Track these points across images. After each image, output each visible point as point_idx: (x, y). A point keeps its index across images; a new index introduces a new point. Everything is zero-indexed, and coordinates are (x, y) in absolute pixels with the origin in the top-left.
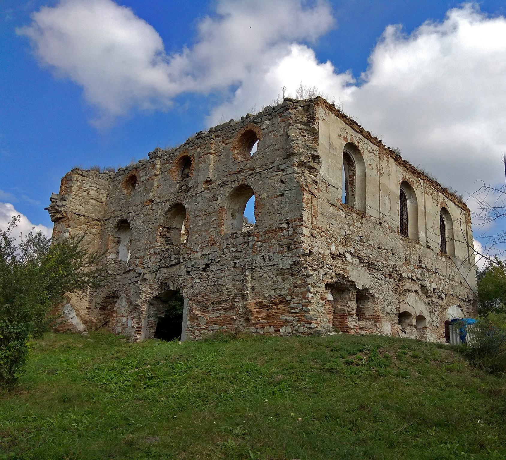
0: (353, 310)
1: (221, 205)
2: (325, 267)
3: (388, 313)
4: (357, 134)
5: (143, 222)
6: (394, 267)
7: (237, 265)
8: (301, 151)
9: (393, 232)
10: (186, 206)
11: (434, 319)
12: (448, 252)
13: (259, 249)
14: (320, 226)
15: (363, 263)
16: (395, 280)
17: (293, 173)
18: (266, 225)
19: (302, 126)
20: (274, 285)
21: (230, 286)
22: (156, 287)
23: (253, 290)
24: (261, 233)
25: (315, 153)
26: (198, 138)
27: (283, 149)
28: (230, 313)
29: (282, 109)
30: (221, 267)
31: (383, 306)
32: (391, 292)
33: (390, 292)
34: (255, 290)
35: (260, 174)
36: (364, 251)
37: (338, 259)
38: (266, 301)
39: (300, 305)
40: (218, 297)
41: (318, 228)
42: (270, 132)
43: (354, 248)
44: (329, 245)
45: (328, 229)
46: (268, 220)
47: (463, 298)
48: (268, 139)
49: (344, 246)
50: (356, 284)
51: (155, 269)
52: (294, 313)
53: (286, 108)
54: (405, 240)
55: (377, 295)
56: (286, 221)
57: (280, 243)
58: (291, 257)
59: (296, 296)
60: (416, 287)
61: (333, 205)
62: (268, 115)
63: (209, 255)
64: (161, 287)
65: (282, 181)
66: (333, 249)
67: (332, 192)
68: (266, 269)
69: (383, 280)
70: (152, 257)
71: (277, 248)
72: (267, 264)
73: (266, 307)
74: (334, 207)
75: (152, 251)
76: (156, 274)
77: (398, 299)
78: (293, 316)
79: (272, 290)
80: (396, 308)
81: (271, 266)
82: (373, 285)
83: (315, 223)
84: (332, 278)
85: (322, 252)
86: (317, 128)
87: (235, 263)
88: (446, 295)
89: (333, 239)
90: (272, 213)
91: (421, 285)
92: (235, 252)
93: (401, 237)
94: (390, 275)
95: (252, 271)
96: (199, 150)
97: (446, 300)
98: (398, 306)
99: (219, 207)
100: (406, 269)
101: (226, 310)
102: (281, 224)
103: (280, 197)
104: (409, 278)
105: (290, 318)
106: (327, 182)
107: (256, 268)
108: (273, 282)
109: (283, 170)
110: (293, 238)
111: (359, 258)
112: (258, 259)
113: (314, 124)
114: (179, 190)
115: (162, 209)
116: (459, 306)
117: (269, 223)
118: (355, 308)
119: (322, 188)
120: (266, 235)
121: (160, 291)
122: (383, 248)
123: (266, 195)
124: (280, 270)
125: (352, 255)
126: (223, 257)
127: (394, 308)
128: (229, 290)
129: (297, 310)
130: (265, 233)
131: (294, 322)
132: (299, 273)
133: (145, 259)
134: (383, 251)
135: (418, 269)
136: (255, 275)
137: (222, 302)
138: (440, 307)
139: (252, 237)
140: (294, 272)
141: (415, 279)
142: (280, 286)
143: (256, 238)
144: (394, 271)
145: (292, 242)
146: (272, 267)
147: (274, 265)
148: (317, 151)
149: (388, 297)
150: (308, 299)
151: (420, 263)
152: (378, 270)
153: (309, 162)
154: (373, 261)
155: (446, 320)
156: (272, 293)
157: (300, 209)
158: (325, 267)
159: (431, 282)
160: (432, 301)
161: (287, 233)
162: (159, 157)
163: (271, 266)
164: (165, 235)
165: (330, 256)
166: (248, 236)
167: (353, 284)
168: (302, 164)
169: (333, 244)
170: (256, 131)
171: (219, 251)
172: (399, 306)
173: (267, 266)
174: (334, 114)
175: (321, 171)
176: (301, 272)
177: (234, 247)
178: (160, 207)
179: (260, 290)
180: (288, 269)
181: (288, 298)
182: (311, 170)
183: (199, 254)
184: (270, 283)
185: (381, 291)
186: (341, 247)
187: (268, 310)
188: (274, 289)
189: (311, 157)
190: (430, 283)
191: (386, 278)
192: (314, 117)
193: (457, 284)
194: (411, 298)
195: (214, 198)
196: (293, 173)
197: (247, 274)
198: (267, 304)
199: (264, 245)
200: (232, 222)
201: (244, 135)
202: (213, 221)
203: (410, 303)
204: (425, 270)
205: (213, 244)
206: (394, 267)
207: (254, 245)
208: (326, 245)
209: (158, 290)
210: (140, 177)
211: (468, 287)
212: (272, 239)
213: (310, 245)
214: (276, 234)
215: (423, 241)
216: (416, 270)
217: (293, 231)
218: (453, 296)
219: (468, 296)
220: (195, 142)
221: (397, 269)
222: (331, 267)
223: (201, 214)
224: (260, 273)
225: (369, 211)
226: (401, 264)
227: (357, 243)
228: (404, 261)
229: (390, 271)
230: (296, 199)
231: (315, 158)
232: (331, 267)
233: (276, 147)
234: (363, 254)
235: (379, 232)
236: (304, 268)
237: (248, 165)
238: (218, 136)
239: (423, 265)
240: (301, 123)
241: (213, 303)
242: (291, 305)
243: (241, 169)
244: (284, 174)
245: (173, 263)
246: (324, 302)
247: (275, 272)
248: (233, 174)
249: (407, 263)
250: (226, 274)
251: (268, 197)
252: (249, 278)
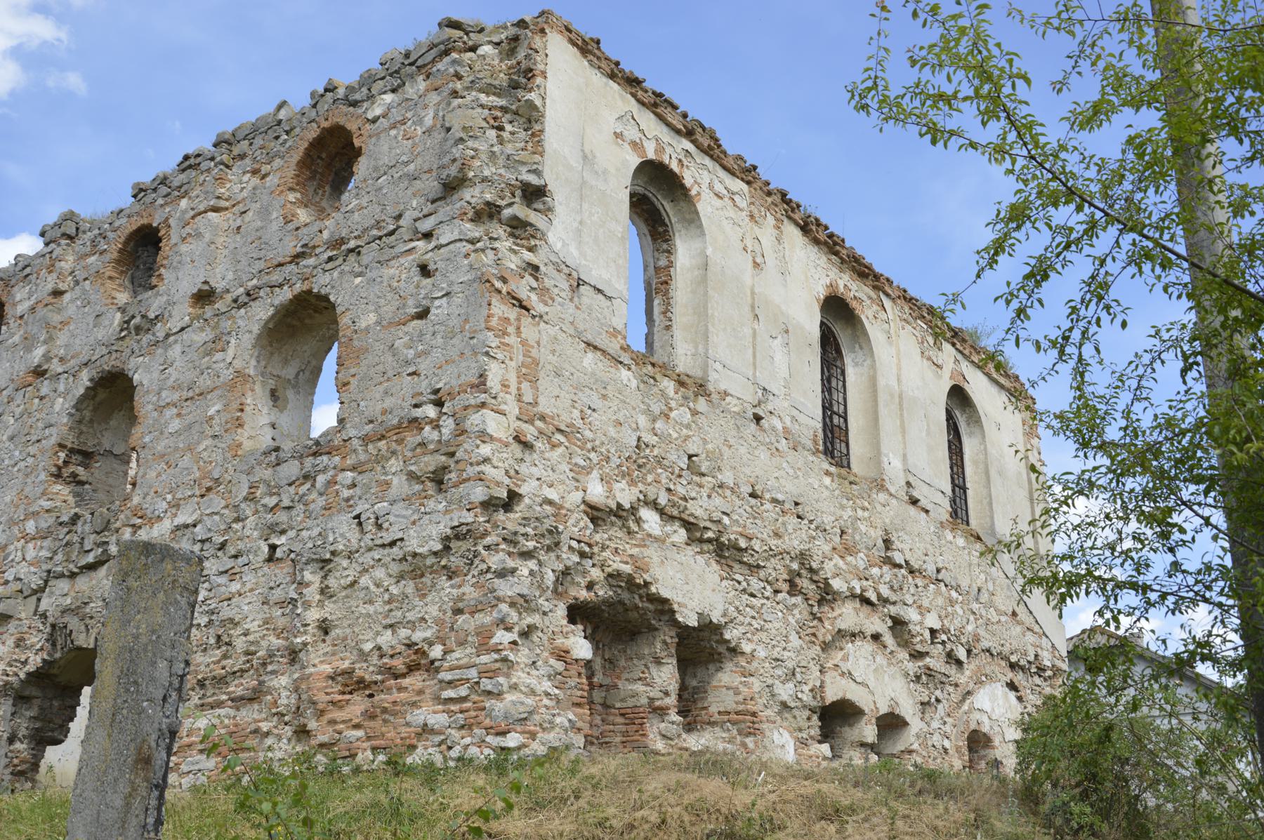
0: (667, 694)
1: (238, 364)
2: (565, 549)
3: (784, 705)
4: (677, 137)
5: (11, 438)
6: (803, 557)
7: (279, 554)
8: (487, 173)
9: (800, 448)
10: (136, 377)
11: (935, 724)
12: (973, 521)
13: (346, 493)
14: (548, 411)
15: (701, 541)
16: (807, 599)
17: (461, 240)
18: (369, 414)
19: (492, 98)
20: (391, 610)
21: (256, 623)
22: (37, 640)
23: (326, 633)
24: (355, 442)
25: (533, 179)
26: (184, 170)
27: (430, 171)
28: (249, 715)
29: (434, 52)
30: (230, 563)
31: (770, 682)
32: (793, 637)
33: (791, 638)
34: (333, 634)
35: (359, 253)
36: (704, 501)
37: (613, 524)
38: (365, 665)
39: (473, 673)
40: (219, 662)
41: (543, 418)
42: (393, 127)
43: (669, 490)
44: (580, 473)
45: (579, 423)
46: (378, 396)
47: (1022, 663)
48: (386, 148)
49: (633, 483)
50: (676, 607)
51: (36, 582)
52: (451, 700)
53: (442, 47)
54: (840, 476)
55: (747, 647)
56: (433, 397)
57: (413, 468)
58: (447, 512)
59: (462, 643)
60: (876, 624)
61: (596, 348)
62: (391, 75)
63: (195, 526)
64: (52, 640)
65: (425, 271)
66: (596, 491)
67: (590, 308)
68: (367, 559)
69: (768, 598)
70: (31, 545)
71: (399, 485)
72: (370, 543)
73: (367, 687)
74: (599, 353)
75: (30, 526)
76: (39, 600)
77: (816, 659)
78: (448, 712)
79: (385, 627)
80: (811, 690)
81: (383, 546)
82: (735, 614)
83: (528, 397)
84: (590, 586)
85: (552, 494)
86: (538, 102)
87: (273, 548)
88: (969, 652)
89: (593, 455)
90: (390, 373)
91: (891, 617)
92: (272, 509)
93: (826, 466)
94: (791, 583)
95: (322, 568)
96: (184, 203)
97: (972, 666)
98: (818, 684)
99: (231, 370)
100: (844, 567)
101: (238, 701)
102: (416, 406)
103: (415, 322)
104: (853, 596)
105: (438, 719)
106: (575, 274)
107: (336, 559)
108: (389, 602)
109: (428, 236)
110: (452, 449)
111: (689, 526)
112: (343, 531)
113: (531, 90)
114: (122, 330)
115: (65, 395)
116: (1012, 686)
117: (379, 407)
118: (673, 687)
119: (556, 291)
120: (370, 446)
121: (49, 654)
122: (767, 496)
123: (372, 318)
124: (409, 558)
125: (661, 512)
126: (237, 531)
127: (806, 688)
128: (251, 638)
129: (463, 691)
130: (366, 440)
131: (453, 732)
132: (472, 564)
133: (9, 554)
134: (768, 506)
135: (881, 567)
136: (332, 582)
137: (228, 679)
138: (951, 689)
139: (325, 458)
140: (455, 561)
141: (874, 598)
142: (412, 613)
143: (337, 459)
144: (804, 572)
145: (451, 462)
146: (387, 550)
147: (393, 544)
148: (536, 172)
149: (786, 654)
150: (498, 651)
151: (887, 549)
152: (750, 566)
153: (510, 205)
154: (732, 537)
155: (973, 726)
156: (386, 639)
157: (476, 354)
158: (565, 549)
160: (929, 669)
161: (435, 435)
162: (70, 238)
163: (383, 546)
164: (74, 475)
165: (585, 512)
166: (315, 454)
167: (664, 607)
168: (488, 212)
169: (595, 474)
170: (352, 126)
171: (226, 511)
172: (822, 682)
173: (370, 550)
174: (599, 68)
175: (551, 237)
176: (476, 561)
177: (271, 495)
178: (61, 388)
179: (348, 631)
180: (435, 553)
181: (436, 652)
182: (517, 232)
183: (166, 525)
184: (379, 606)
185: (763, 636)
186: (623, 485)
187: (371, 696)
188: (391, 626)
189: (518, 193)
190: (921, 614)
191: (776, 592)
192: (531, 70)
193: (1003, 619)
194: (859, 656)
195: (218, 343)
196: (461, 240)
197: (308, 576)
198: (367, 677)
199: (363, 479)
200: (273, 419)
201: (317, 144)
202: (211, 418)
203: (855, 674)
204: (903, 571)
205: (209, 489)
206: (803, 557)
207: (332, 482)
208: (572, 474)
209: (42, 649)
210: (15, 305)
211: (1037, 628)
212: (388, 459)
213: (512, 473)
214: (400, 442)
215: (896, 484)
216: (875, 571)
217: (453, 426)
218: (992, 655)
219: (1036, 656)
220: (176, 183)
221: (814, 565)
222: (587, 549)
223: (176, 396)
224: (346, 573)
225: (718, 380)
226: (827, 548)
227: (680, 476)
228: (837, 539)
229: (791, 572)
230: (466, 321)
231: (534, 194)
232: (587, 549)
233: (412, 167)
234: (699, 512)
235: (754, 444)
236: (487, 548)
237: (326, 234)
238: (242, 157)
239: (898, 558)
240: (489, 90)
241: (201, 684)
242: (442, 675)
243: (303, 246)
244: (433, 244)
245: (90, 558)
246: (560, 666)
247: (395, 568)
248: (280, 265)
249: (849, 550)
250: (244, 584)
251: (378, 323)
252: (312, 593)
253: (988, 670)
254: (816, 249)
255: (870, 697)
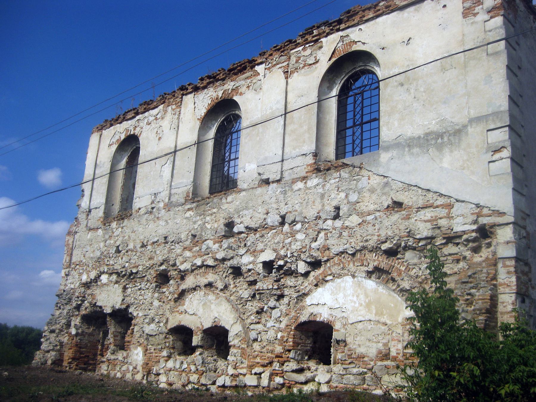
66: (85, 278)
141: (210, 262)
155: (303, 318)
159: (255, 253)
190: (255, 256)
253: (335, 269)
254: (206, 90)
255: (199, 320)
